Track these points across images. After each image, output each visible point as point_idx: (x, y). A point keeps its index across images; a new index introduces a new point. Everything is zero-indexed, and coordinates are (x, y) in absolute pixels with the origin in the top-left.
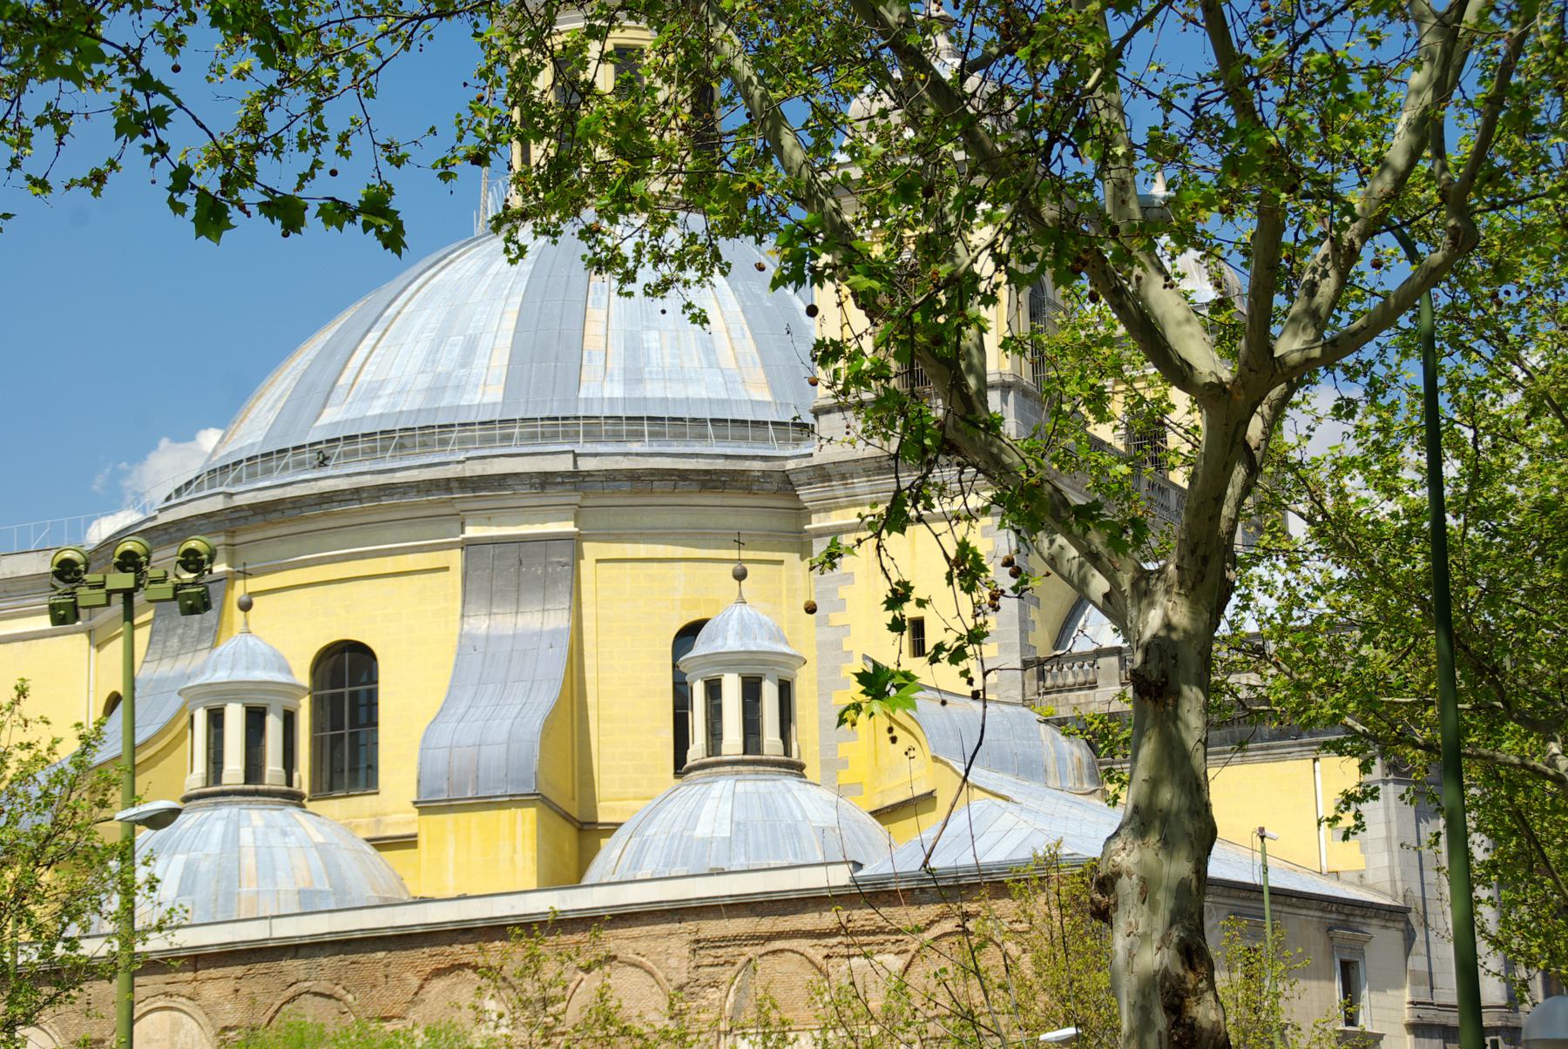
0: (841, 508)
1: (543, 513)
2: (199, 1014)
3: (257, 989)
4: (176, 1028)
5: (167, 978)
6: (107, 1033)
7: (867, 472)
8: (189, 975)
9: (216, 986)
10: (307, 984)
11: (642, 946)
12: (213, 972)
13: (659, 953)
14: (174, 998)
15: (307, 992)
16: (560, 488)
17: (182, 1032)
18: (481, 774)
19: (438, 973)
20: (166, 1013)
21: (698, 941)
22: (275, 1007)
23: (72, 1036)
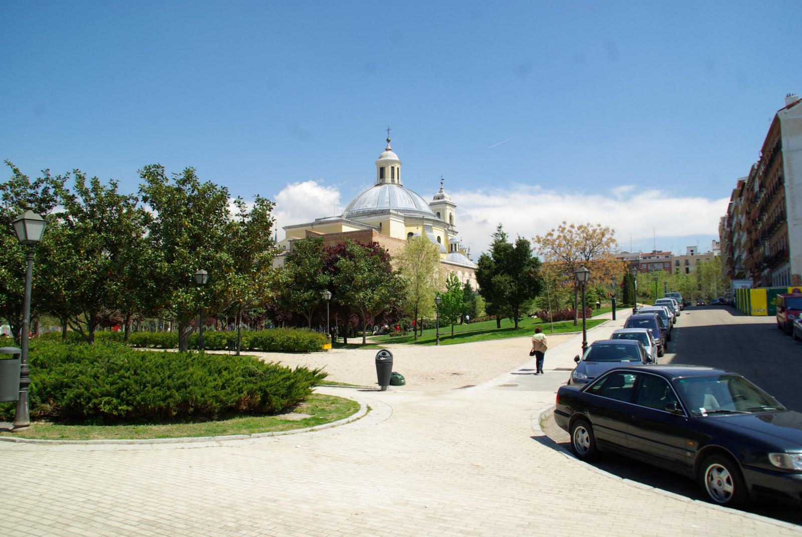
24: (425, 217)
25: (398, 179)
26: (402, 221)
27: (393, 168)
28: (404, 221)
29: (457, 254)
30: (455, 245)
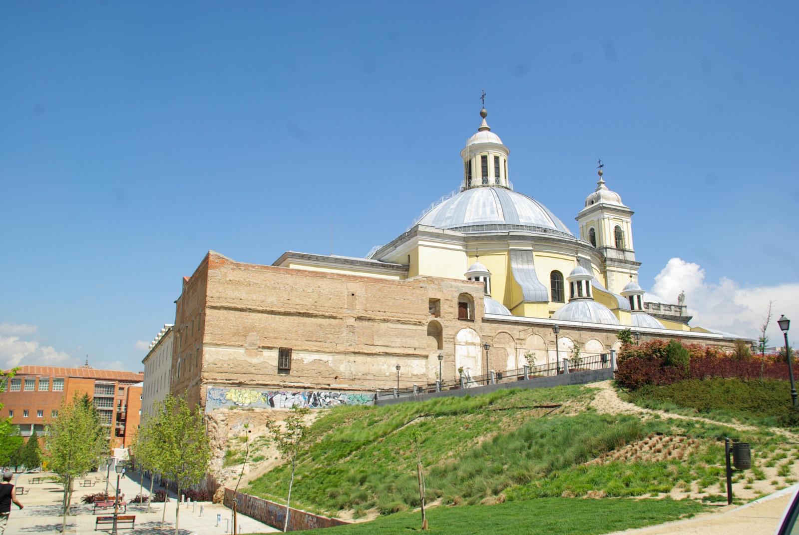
1: (587, 254)
24: (511, 234)
25: (497, 175)
26: (461, 248)
27: (484, 159)
28: (466, 246)
29: (590, 304)
30: (579, 283)
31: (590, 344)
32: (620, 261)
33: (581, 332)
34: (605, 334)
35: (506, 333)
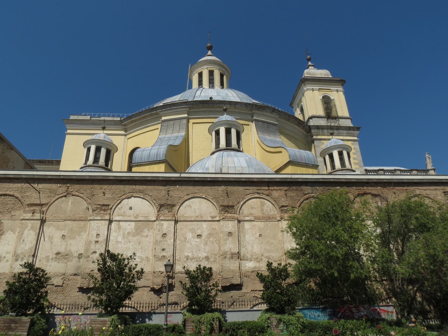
0: (320, 135)
2: (272, 201)
3: (292, 194)
4: (262, 205)
5: (258, 188)
6: (235, 204)
7: (327, 129)
8: (266, 188)
9: (277, 192)
10: (312, 194)
11: (428, 192)
12: (276, 188)
13: (434, 195)
14: (261, 195)
15: (312, 197)
16: (276, 113)
17: (265, 206)
18: (306, 159)
19: (359, 195)
20: (258, 199)
21: (445, 192)
22: (301, 201)
23: (221, 204)
31: (189, 206)
32: (331, 128)
33: (172, 188)
34: (223, 188)
35: (9, 195)
